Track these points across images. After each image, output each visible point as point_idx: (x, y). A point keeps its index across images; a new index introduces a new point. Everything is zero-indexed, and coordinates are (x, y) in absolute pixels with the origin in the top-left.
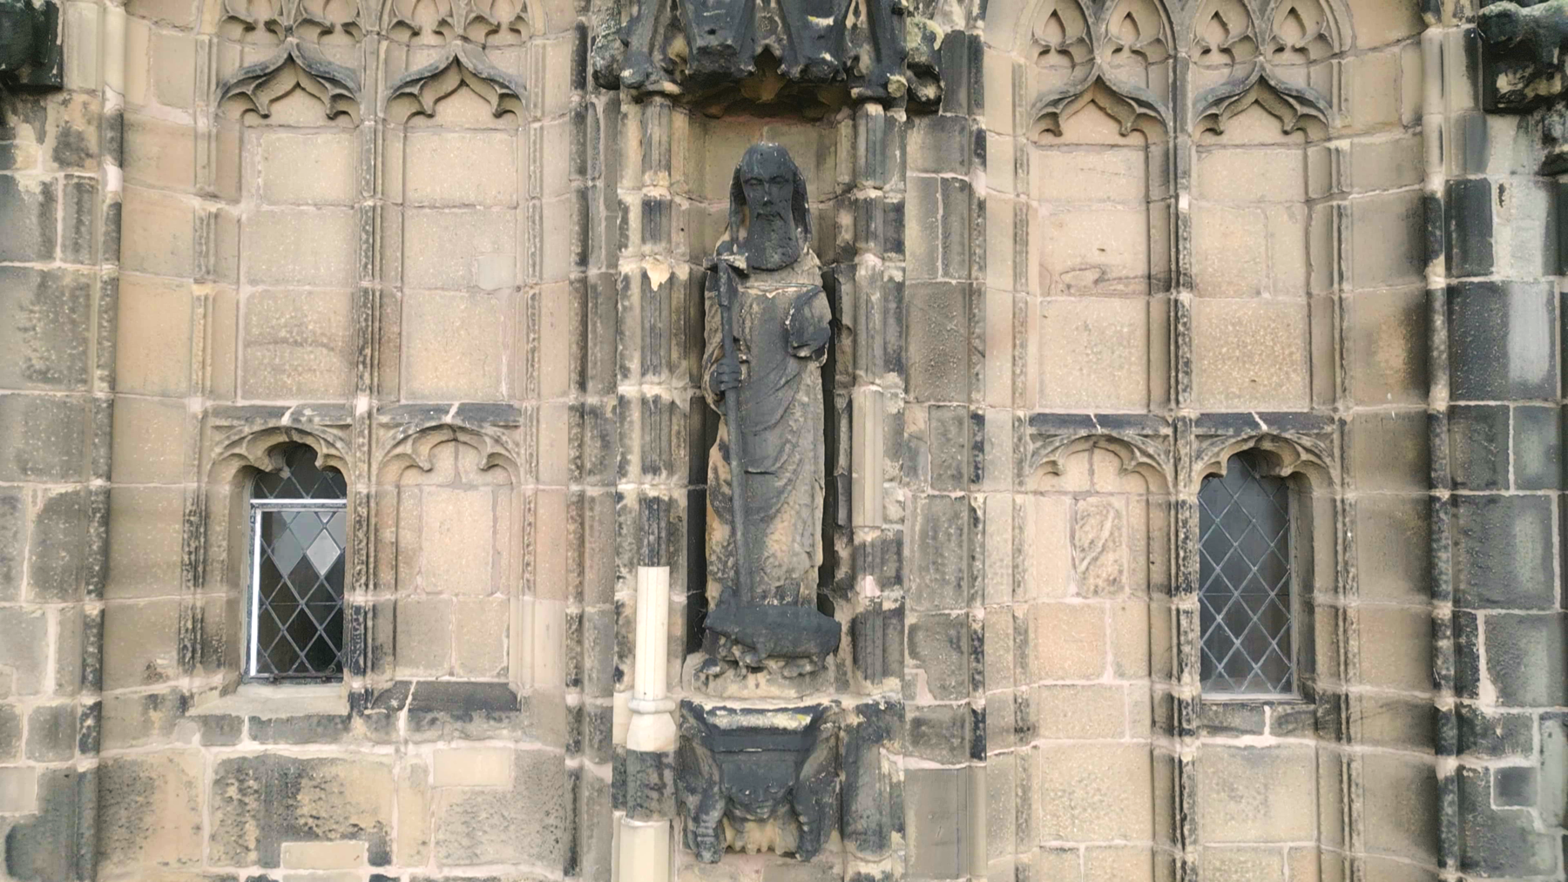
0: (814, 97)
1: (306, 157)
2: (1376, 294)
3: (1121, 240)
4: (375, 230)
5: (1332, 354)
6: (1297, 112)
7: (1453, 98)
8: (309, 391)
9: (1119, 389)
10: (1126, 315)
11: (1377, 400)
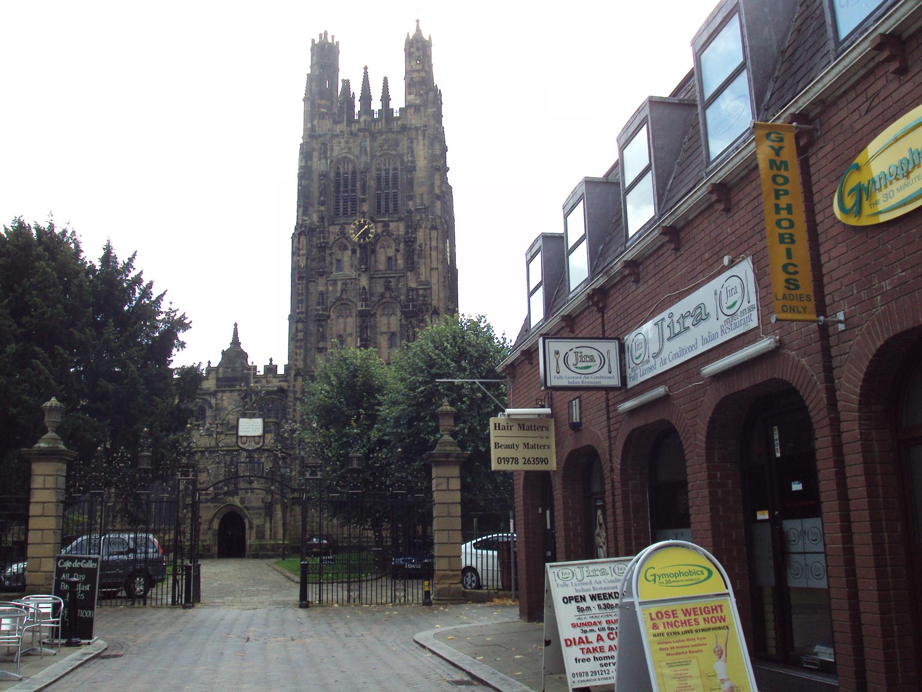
0: (366, 316)
1: (341, 320)
3: (386, 322)
4: (345, 323)
8: (341, 332)
9: (386, 330)
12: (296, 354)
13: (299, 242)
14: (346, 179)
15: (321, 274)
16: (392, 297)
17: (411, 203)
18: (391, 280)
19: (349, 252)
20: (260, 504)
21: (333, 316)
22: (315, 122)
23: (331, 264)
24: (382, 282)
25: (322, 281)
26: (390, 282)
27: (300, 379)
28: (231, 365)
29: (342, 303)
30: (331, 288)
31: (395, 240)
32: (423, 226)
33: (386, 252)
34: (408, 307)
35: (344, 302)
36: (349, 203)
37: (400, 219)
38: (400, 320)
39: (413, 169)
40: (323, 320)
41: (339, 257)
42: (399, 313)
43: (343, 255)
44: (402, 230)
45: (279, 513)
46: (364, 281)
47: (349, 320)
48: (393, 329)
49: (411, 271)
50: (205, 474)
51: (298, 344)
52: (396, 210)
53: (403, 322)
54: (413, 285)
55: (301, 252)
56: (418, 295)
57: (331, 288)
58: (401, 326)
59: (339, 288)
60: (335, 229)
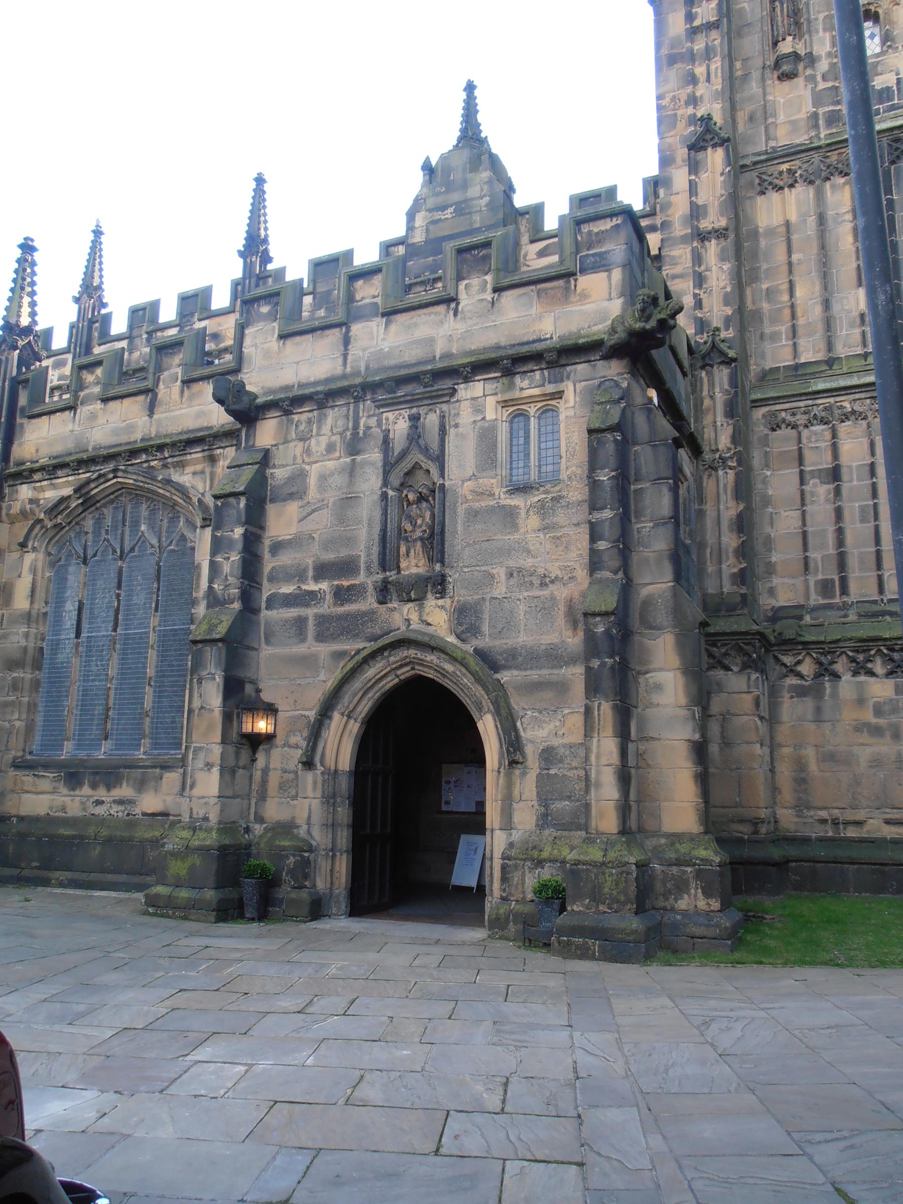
12: (693, 80)
27: (716, 158)
28: (456, 197)
45: (666, 681)
50: (293, 508)
51: (699, 46)
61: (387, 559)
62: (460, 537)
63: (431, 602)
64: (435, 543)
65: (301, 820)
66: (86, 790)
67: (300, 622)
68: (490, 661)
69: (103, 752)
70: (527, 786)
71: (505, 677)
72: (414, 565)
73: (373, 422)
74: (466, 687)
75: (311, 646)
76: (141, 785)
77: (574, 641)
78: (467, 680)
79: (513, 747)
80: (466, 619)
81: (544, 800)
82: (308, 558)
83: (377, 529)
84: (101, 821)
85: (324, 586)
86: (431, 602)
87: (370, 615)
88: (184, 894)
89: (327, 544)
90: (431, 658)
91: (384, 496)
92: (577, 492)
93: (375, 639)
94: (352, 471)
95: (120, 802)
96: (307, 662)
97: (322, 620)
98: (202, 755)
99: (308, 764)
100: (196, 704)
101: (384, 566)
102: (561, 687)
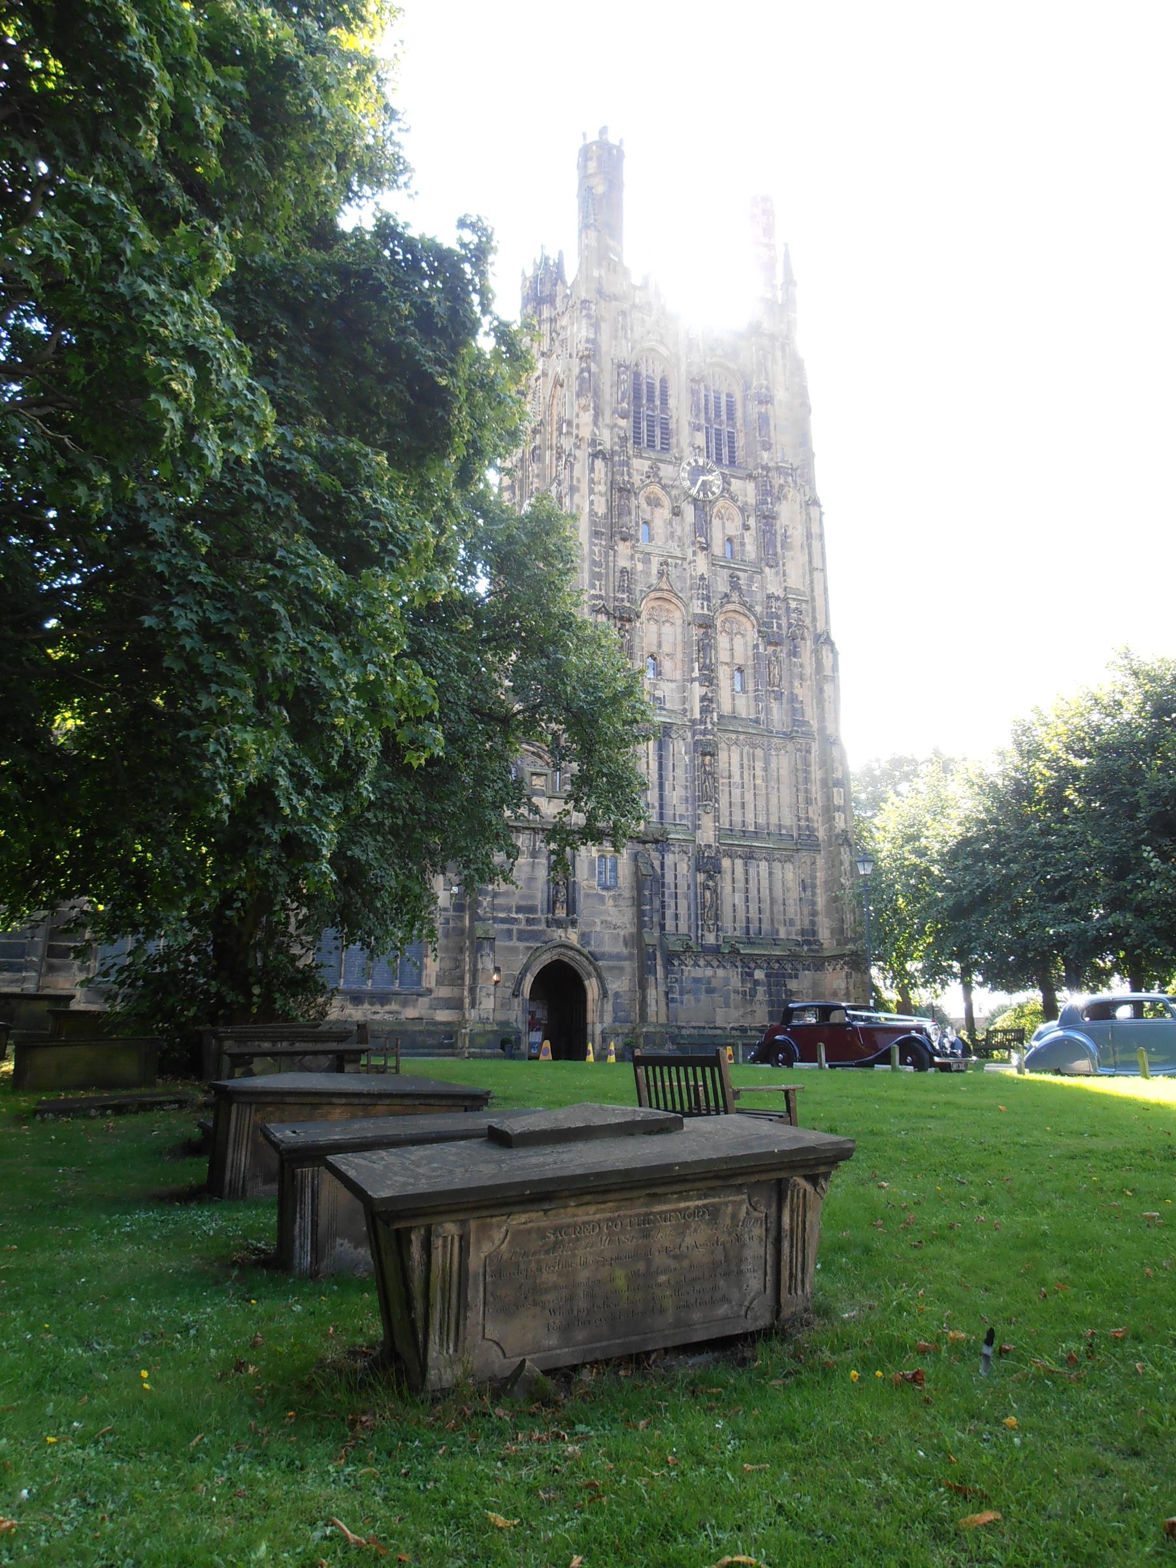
1: (653, 627)
2: (750, 654)
4: (660, 635)
5: (747, 659)
6: (743, 636)
7: (756, 635)
8: (654, 649)
9: (728, 660)
10: (729, 653)
11: (750, 663)
13: (592, 470)
14: (650, 387)
15: (624, 540)
16: (744, 604)
17: (765, 455)
18: (740, 574)
19: (664, 513)
20: (621, 949)
21: (644, 616)
22: (603, 274)
23: (637, 524)
24: (725, 573)
25: (623, 548)
26: (738, 579)
29: (666, 596)
30: (640, 567)
31: (742, 510)
32: (790, 496)
33: (724, 528)
34: (769, 625)
35: (665, 595)
36: (658, 431)
37: (750, 477)
38: (756, 646)
39: (766, 400)
40: (630, 620)
41: (648, 517)
42: (752, 635)
43: (652, 514)
44: (751, 499)
46: (702, 565)
47: (667, 629)
48: (739, 660)
49: (771, 567)
52: (732, 461)
53: (761, 649)
54: (774, 589)
55: (597, 488)
56: (788, 609)
57: (640, 567)
58: (757, 656)
59: (654, 571)
60: (640, 465)
61: (551, 906)
62: (582, 904)
63: (570, 930)
64: (571, 907)
65: (512, 1019)
66: (366, 1006)
67: (510, 932)
68: (594, 957)
69: (369, 985)
70: (609, 1007)
71: (600, 963)
72: (561, 913)
73: (543, 845)
74: (582, 965)
75: (514, 943)
76: (404, 1004)
77: (625, 951)
78: (586, 963)
79: (604, 994)
80: (584, 937)
81: (615, 1011)
82: (514, 902)
83: (546, 895)
84: (379, 1023)
85: (520, 916)
86: (570, 930)
87: (543, 932)
88: (488, 1051)
89: (522, 897)
90: (571, 953)
91: (548, 881)
92: (627, 894)
93: (546, 943)
94: (533, 865)
95: (391, 1013)
96: (513, 950)
97: (520, 932)
98: (484, 990)
99: (515, 994)
100: (480, 966)
101: (548, 912)
102: (621, 969)
